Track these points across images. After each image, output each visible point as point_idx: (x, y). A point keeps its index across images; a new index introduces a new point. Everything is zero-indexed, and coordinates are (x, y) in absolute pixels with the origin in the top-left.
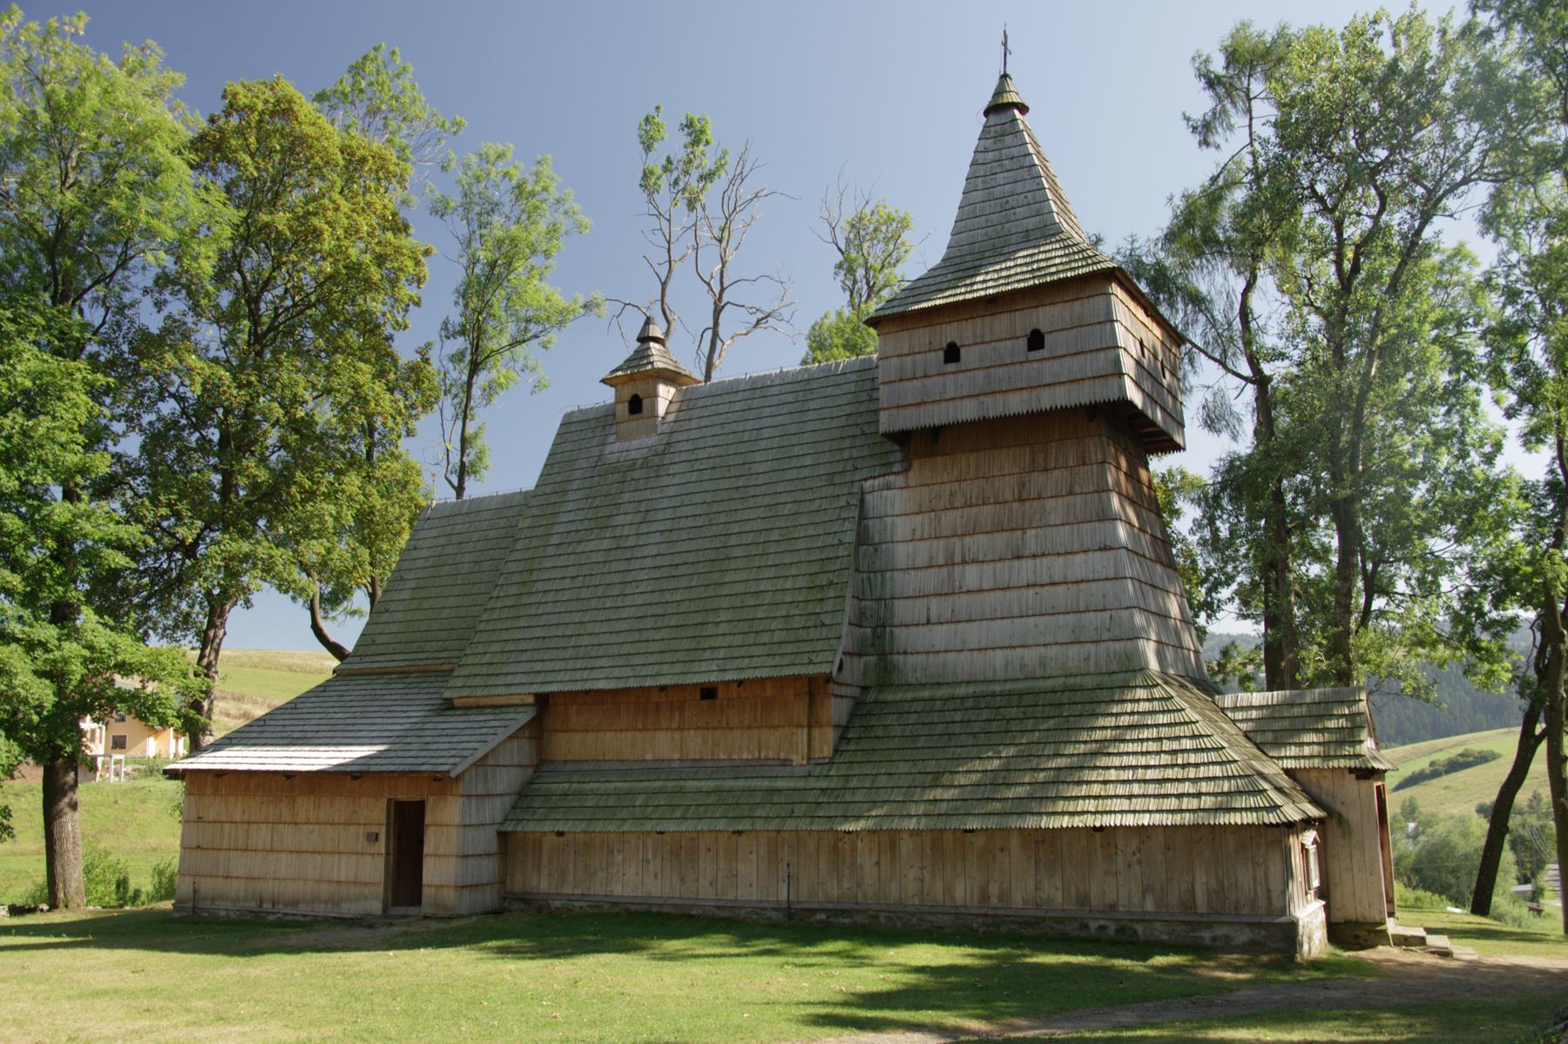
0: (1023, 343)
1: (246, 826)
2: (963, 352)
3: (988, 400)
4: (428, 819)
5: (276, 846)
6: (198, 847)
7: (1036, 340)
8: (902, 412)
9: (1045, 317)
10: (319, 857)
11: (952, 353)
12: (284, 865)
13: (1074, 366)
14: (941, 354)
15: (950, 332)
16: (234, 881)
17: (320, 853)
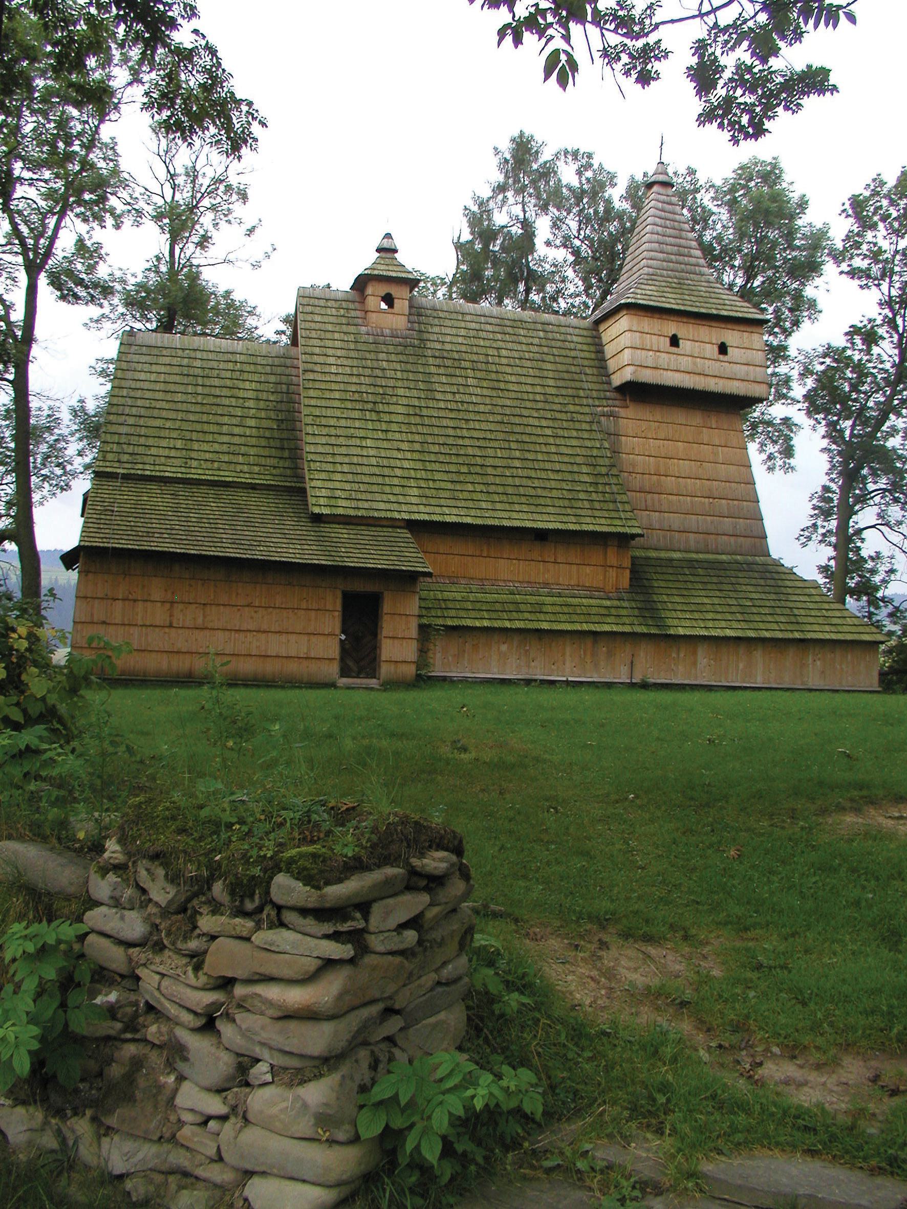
0: (716, 349)
1: (168, 606)
2: (681, 342)
3: (697, 378)
4: (387, 606)
5: (210, 625)
6: (104, 623)
7: (723, 349)
8: (644, 370)
9: (731, 336)
10: (263, 636)
11: (675, 341)
12: (218, 642)
13: (741, 370)
14: (668, 340)
15: (672, 327)
16: (154, 655)
17: (264, 632)
